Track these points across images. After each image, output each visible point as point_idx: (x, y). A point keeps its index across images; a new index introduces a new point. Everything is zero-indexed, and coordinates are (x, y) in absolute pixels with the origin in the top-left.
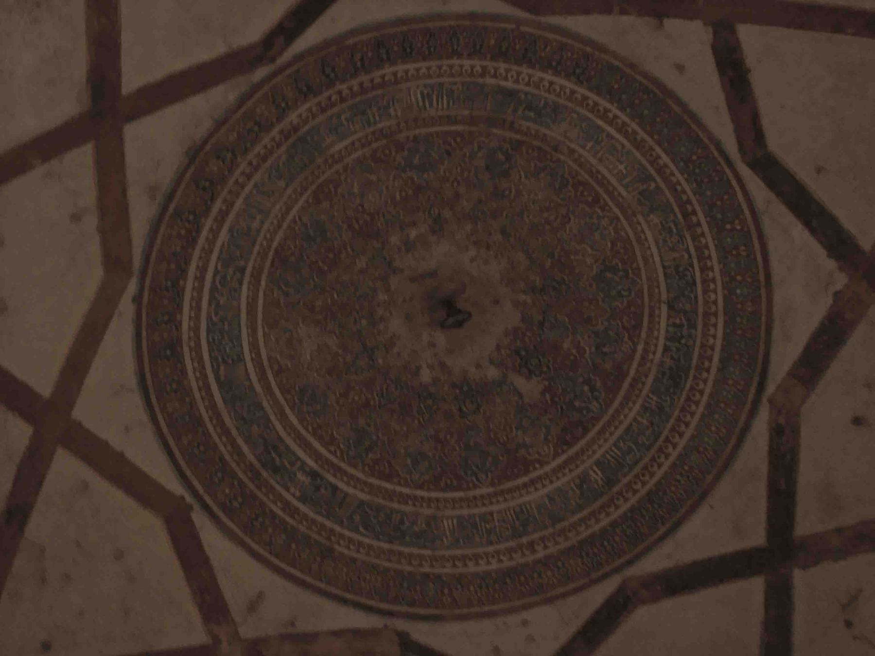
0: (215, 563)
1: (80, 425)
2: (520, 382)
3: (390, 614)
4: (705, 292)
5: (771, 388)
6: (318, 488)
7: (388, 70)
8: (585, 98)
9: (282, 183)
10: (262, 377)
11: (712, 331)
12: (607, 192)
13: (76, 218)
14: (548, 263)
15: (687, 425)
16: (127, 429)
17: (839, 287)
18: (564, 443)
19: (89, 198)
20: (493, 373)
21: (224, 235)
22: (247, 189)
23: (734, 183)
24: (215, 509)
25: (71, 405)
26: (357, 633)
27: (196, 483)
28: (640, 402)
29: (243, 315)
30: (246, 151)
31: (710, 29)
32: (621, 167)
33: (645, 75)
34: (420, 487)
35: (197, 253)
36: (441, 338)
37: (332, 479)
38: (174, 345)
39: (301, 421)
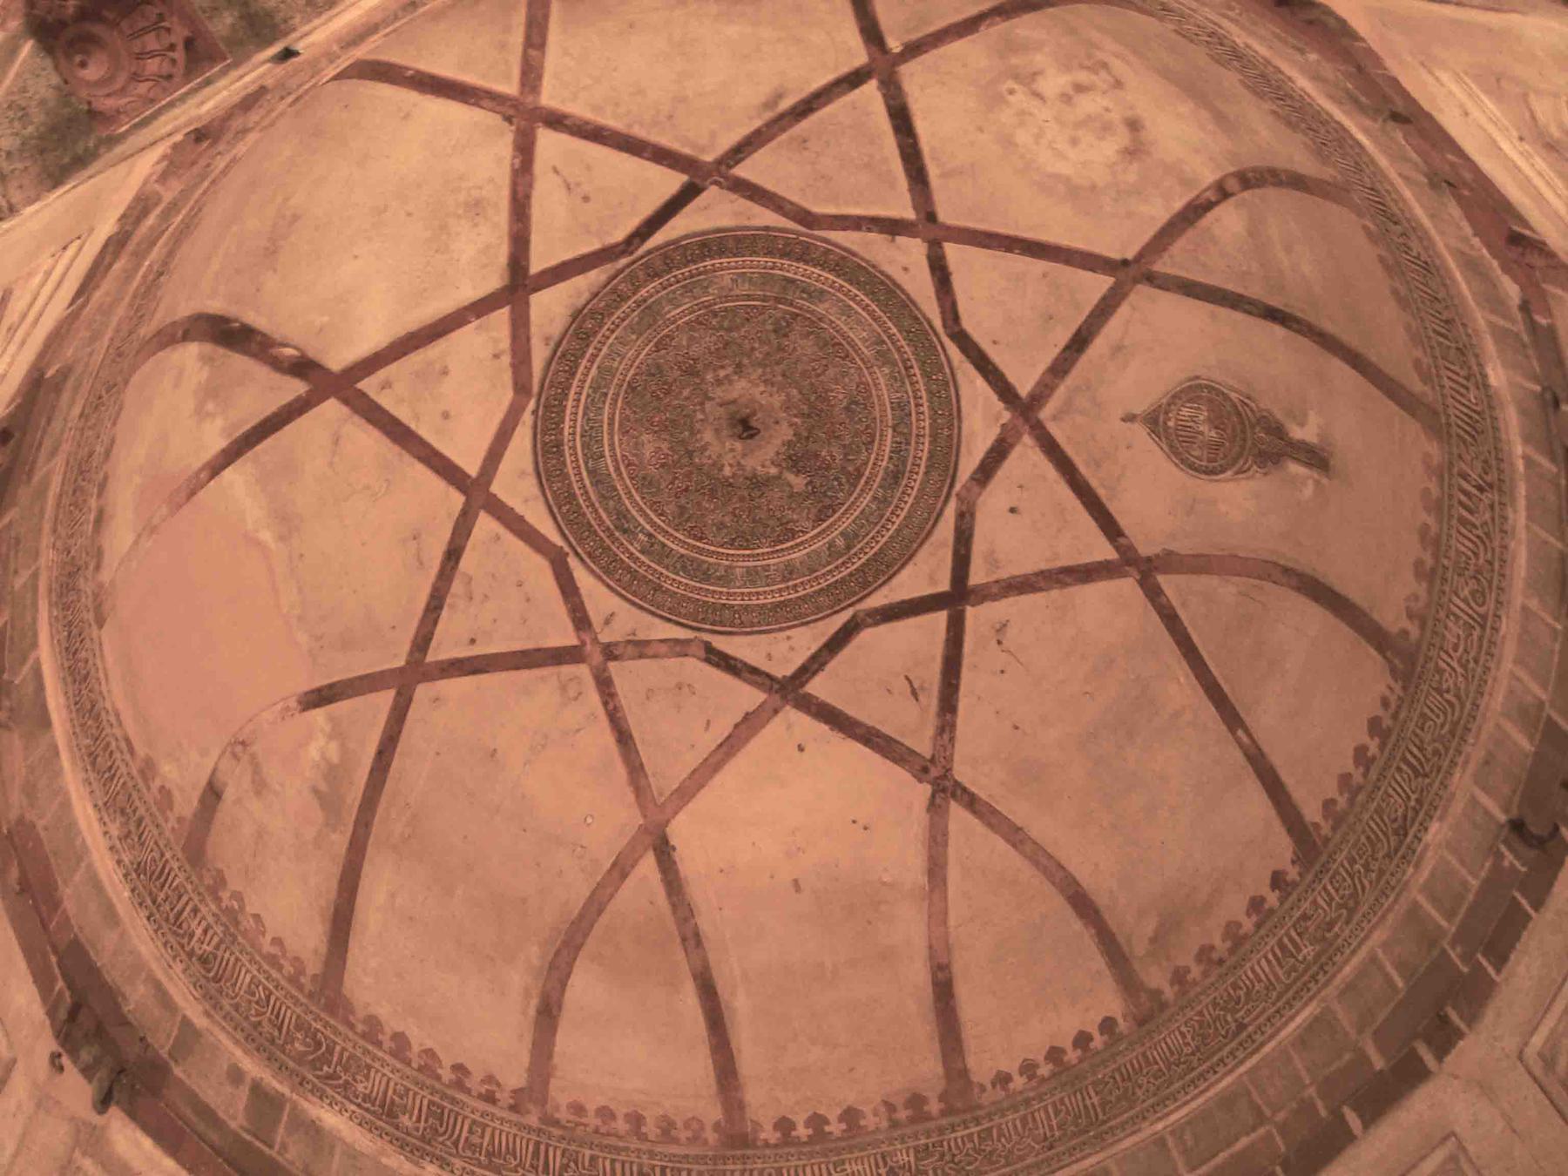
0: (583, 591)
1: (495, 496)
2: (791, 477)
3: (699, 629)
4: (918, 420)
5: (958, 487)
6: (652, 545)
7: (708, 263)
8: (842, 286)
9: (634, 337)
10: (617, 469)
11: (921, 447)
12: (856, 351)
13: (496, 356)
14: (813, 398)
15: (902, 509)
16: (526, 501)
17: (1003, 421)
18: (820, 520)
19: (505, 344)
20: (773, 471)
21: (594, 371)
22: (610, 341)
23: (939, 348)
24: (584, 556)
25: (489, 483)
26: (677, 641)
27: (572, 539)
28: (871, 493)
29: (605, 427)
30: (612, 314)
31: (926, 245)
32: (865, 334)
33: (882, 273)
34: (722, 546)
35: (575, 383)
36: (738, 445)
37: (662, 539)
38: (559, 445)
39: (643, 498)
